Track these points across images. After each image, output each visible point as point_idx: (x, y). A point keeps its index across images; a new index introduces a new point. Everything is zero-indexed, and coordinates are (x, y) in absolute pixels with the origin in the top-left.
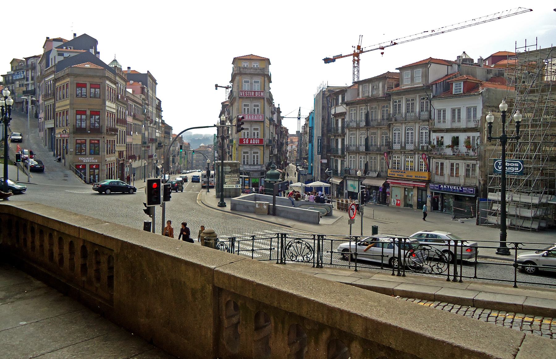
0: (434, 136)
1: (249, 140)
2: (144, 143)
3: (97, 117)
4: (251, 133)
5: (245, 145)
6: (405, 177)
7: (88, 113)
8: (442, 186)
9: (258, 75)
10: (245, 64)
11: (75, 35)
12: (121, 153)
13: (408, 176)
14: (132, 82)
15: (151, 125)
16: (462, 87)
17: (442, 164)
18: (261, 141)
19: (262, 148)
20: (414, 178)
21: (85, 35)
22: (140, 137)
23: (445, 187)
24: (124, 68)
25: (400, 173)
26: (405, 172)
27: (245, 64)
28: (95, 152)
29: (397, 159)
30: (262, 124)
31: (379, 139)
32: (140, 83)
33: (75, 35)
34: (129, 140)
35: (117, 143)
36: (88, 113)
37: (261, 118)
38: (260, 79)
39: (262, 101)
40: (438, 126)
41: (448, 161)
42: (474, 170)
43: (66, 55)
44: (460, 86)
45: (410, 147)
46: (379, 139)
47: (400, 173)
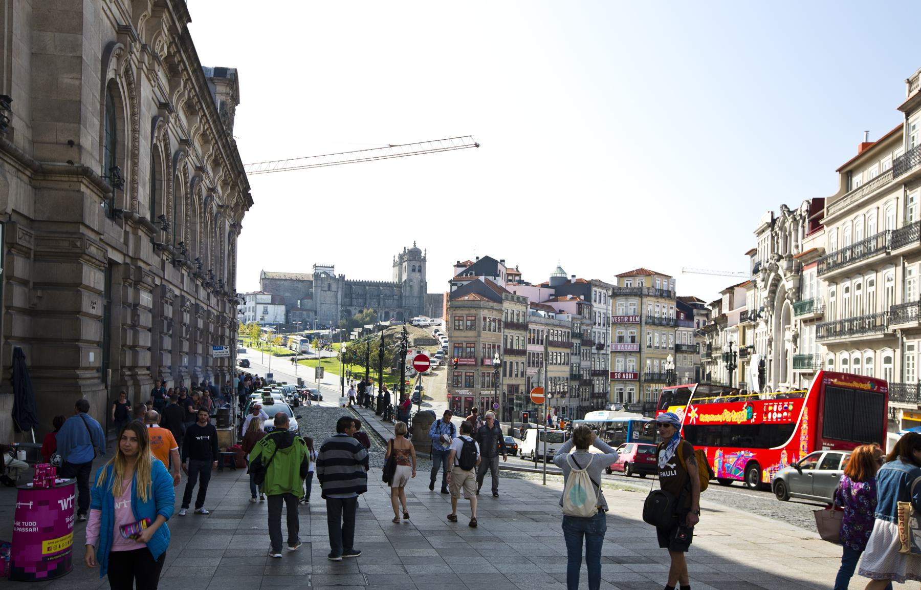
1: (622, 374)
2: (575, 377)
3: (473, 349)
4: (625, 366)
5: (617, 380)
7: (464, 345)
9: (635, 295)
10: (627, 282)
11: (477, 258)
12: (514, 389)
14: (569, 296)
15: (603, 352)
18: (635, 375)
19: (638, 384)
21: (487, 257)
22: (567, 368)
24: (569, 278)
27: (627, 282)
28: (469, 385)
30: (638, 355)
32: (582, 297)
33: (477, 258)
34: (532, 371)
35: (505, 375)
36: (464, 345)
37: (635, 347)
38: (635, 301)
39: (639, 327)
43: (459, 284)
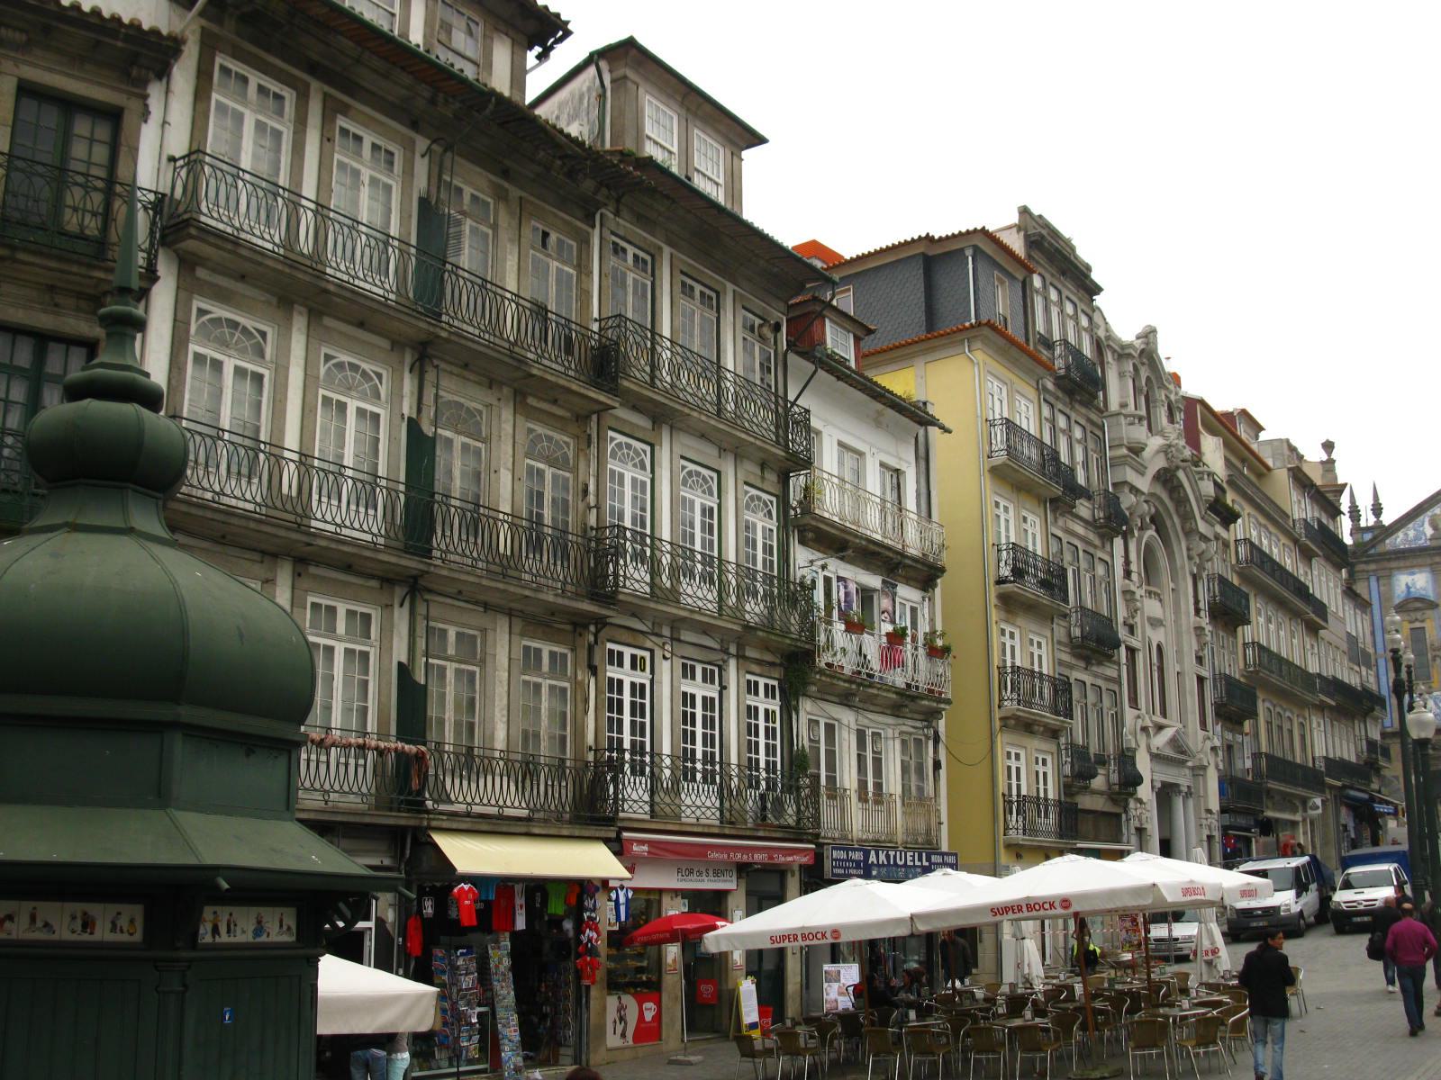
29: (627, 676)
31: (505, 477)
46: (505, 477)
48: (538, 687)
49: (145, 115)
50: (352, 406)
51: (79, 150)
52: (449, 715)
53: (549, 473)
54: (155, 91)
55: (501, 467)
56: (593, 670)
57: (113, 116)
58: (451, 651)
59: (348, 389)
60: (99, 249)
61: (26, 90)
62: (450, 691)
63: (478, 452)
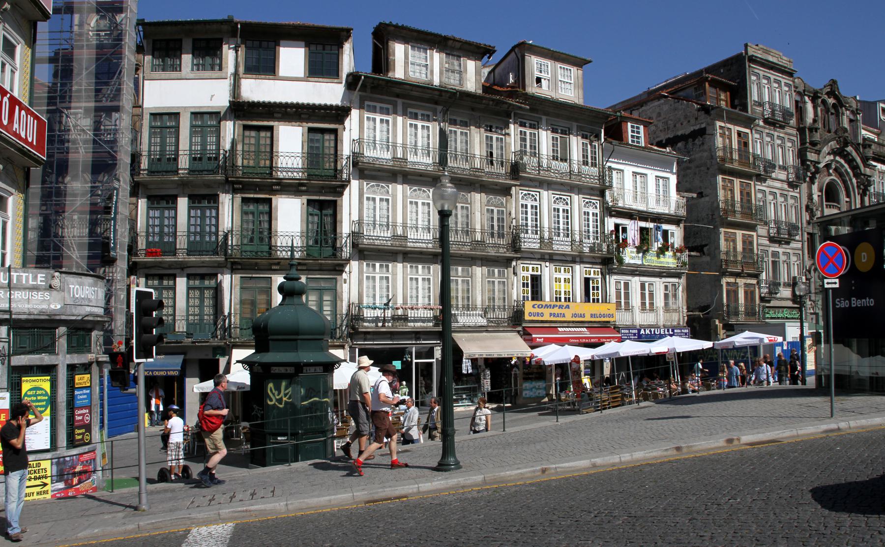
0: (611, 223)
6: (568, 318)
8: (642, 332)
13: (575, 315)
16: (642, 134)
17: (626, 285)
20: (588, 318)
23: (648, 332)
25: (556, 310)
26: (568, 307)
31: (478, 215)
40: (628, 202)
41: (637, 279)
42: (675, 296)
44: (638, 133)
45: (562, 246)
46: (478, 215)
47: (556, 310)
48: (493, 282)
49: (344, 128)
50: (420, 202)
51: (327, 144)
52: (460, 295)
53: (495, 210)
54: (347, 123)
55: (476, 212)
56: (515, 274)
57: (335, 132)
58: (460, 274)
59: (418, 198)
60: (337, 172)
61: (310, 130)
62: (460, 287)
63: (467, 208)
